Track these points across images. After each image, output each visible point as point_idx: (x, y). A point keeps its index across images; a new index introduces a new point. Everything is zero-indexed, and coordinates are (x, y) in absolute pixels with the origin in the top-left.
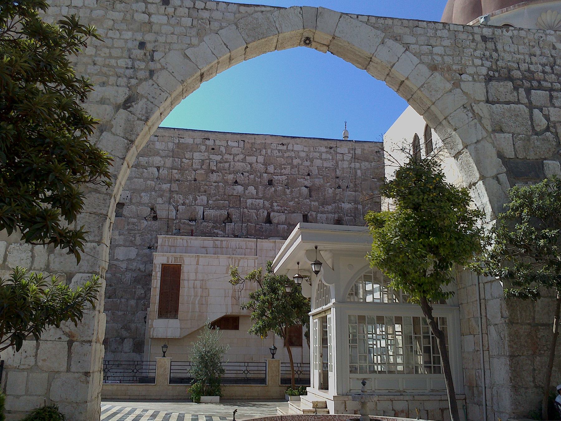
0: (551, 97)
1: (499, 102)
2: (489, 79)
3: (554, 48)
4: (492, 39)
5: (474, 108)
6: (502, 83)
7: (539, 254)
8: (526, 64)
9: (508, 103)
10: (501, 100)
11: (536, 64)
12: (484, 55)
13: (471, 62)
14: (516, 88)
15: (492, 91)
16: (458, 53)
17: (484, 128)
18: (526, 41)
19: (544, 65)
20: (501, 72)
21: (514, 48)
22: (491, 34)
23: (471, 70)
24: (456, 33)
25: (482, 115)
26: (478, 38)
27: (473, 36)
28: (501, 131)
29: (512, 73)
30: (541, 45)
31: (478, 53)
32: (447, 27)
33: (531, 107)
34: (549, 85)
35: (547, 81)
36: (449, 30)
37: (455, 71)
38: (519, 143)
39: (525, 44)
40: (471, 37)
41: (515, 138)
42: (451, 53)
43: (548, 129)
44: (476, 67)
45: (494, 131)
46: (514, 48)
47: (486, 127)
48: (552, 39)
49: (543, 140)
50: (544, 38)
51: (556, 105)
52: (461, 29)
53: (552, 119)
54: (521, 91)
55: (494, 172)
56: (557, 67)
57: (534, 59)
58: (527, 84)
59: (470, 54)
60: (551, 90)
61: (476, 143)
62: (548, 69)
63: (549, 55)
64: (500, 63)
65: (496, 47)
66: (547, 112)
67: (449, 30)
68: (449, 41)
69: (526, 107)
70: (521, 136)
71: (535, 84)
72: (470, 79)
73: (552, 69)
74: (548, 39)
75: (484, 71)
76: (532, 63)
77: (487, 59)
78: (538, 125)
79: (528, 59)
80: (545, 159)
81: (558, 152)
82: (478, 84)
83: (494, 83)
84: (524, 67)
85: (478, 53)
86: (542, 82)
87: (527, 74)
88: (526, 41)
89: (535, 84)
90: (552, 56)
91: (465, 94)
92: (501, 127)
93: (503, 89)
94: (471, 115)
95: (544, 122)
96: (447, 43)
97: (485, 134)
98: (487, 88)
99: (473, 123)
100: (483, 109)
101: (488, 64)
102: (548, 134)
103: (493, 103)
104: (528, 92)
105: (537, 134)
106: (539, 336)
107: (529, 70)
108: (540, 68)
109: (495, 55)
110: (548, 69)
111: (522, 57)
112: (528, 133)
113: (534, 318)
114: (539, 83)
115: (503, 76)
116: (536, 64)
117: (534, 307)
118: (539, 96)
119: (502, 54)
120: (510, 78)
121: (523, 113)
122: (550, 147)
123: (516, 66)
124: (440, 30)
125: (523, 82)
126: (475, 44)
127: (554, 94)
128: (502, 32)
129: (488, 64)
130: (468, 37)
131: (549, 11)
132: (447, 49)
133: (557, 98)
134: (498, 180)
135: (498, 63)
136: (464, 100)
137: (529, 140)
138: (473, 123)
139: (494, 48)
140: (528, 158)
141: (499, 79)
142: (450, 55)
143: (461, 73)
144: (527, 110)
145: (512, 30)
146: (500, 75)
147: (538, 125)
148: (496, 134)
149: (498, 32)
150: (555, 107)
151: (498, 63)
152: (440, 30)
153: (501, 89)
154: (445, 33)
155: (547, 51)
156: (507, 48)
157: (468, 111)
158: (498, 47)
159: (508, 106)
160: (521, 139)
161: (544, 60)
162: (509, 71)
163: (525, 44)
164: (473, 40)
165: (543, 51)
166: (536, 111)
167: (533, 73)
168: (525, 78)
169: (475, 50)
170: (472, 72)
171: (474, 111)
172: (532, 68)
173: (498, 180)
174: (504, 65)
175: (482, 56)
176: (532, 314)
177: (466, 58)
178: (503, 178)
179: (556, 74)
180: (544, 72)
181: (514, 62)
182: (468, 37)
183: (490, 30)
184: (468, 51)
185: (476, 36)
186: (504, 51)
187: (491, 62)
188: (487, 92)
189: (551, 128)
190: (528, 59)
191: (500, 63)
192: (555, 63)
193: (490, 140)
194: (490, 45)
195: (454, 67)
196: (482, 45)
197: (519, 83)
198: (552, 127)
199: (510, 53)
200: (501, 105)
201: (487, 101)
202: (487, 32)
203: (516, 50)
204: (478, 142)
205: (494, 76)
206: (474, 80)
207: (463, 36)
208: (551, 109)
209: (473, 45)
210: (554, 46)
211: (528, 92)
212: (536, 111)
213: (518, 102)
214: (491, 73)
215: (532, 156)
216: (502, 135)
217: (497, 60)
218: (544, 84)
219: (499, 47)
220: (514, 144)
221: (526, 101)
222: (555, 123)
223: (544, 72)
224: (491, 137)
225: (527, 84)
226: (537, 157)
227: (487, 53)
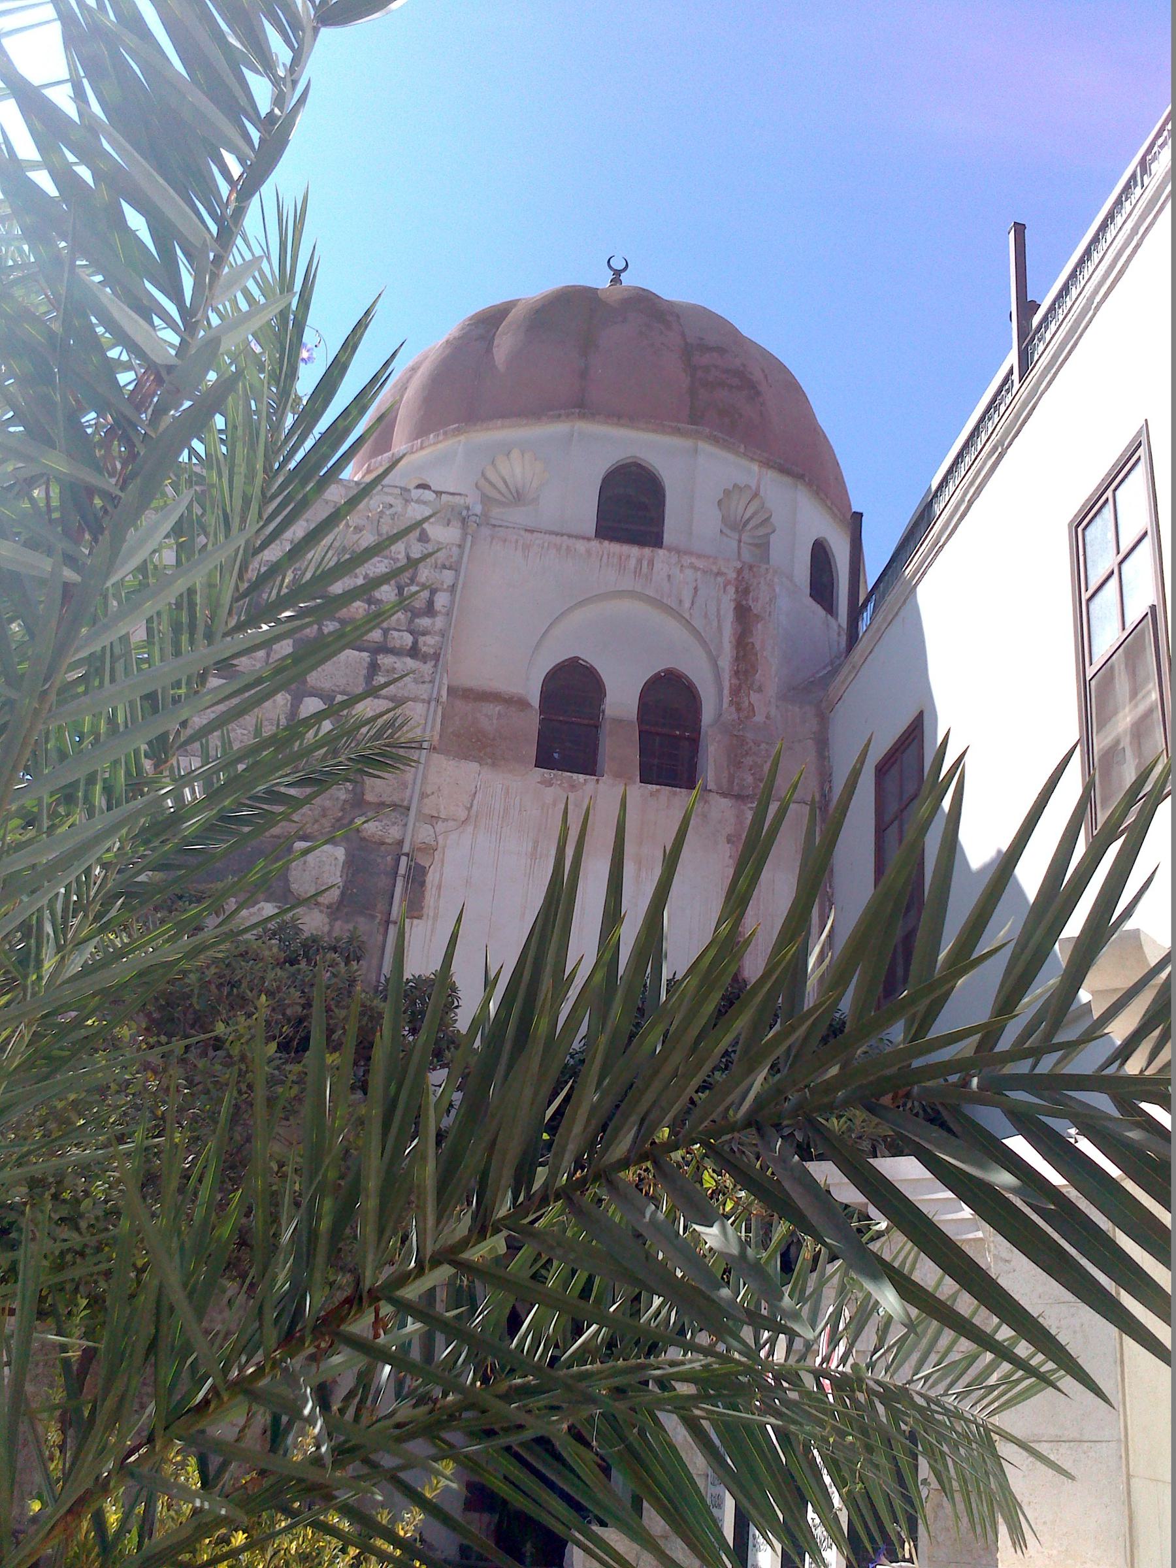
0: (374, 668)
50: (398, 508)
60: (383, 648)
127: (385, 660)
131: (515, 453)
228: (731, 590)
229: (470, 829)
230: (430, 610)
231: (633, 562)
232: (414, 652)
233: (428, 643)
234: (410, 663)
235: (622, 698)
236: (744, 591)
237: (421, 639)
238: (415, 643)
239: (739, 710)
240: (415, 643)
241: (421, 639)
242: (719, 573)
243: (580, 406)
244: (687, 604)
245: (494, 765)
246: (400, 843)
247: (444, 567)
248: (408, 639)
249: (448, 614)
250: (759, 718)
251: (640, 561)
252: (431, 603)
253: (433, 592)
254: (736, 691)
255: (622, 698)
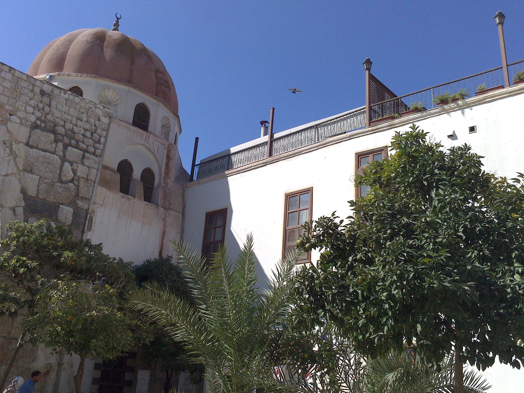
0: (84, 156)
1: (37, 148)
2: (35, 126)
3: (99, 120)
4: (50, 95)
5: (13, 146)
6: (45, 133)
7: (19, 279)
8: (71, 125)
9: (45, 151)
10: (39, 147)
11: (80, 127)
12: (37, 106)
13: (23, 108)
14: (56, 141)
15: (34, 137)
16: (14, 96)
17: (16, 165)
18: (78, 107)
19: (86, 130)
20: (48, 124)
21: (65, 108)
22: (50, 91)
23: (21, 114)
24: (19, 80)
25: (18, 154)
26: (37, 90)
27: (33, 87)
28: (31, 172)
29: (56, 128)
30: (89, 114)
31: (32, 103)
32: (13, 72)
33: (64, 159)
34: (85, 147)
35: (84, 143)
36: (13, 75)
37: (7, 111)
38: (43, 186)
39: (76, 108)
40: (31, 87)
41: (42, 181)
42: (8, 94)
43: (72, 181)
44: (27, 113)
45: (25, 170)
46: (65, 108)
47: (19, 165)
48: (99, 112)
49: (65, 188)
50: (93, 109)
51: (86, 164)
52: (25, 77)
53: (78, 174)
54: (60, 145)
55: (13, 204)
56: (96, 135)
57: (79, 123)
58: (66, 140)
59: (25, 101)
60: (85, 151)
61: (5, 176)
62: (88, 134)
63: (93, 124)
64: (49, 117)
65: (50, 102)
66: (76, 168)
67: (13, 75)
68: (10, 84)
69: (60, 158)
70: (47, 180)
71: (73, 142)
72: (18, 121)
73: (92, 135)
74: (96, 111)
75: (33, 118)
76: (76, 126)
77: (39, 110)
78: (65, 176)
79: (74, 121)
80: (62, 204)
81: (75, 201)
82: (23, 128)
83: (38, 131)
84: (69, 126)
85: (32, 103)
86: (80, 143)
87: (69, 133)
88: (78, 107)
89: (73, 142)
90: (95, 126)
91: (9, 132)
92: (32, 169)
93: (45, 138)
94: (8, 151)
95: (71, 175)
96: (7, 84)
97: (15, 170)
98: (30, 133)
99: (7, 158)
100: (21, 150)
101: (39, 114)
102: (71, 184)
103: (32, 147)
104: (66, 146)
105: (62, 182)
106: (10, 349)
107: (72, 131)
108: (83, 131)
109: (47, 109)
110: (88, 134)
111: (70, 118)
112: (54, 180)
113: (10, 333)
114: (77, 142)
115: (48, 127)
116: (80, 127)
117: (12, 323)
118: (73, 153)
119: (54, 110)
120: (54, 132)
121: (55, 162)
122: (69, 195)
123: (62, 123)
124: (5, 72)
125: (63, 139)
126: (32, 94)
127: (87, 155)
128: (60, 93)
129: (39, 114)
130: (28, 86)
131: (111, 90)
132: (6, 90)
133: (88, 159)
134: (14, 211)
135: (48, 116)
136: (7, 137)
137: (53, 186)
138: (7, 158)
139: (48, 103)
140: (47, 199)
141: (44, 129)
142: (7, 96)
143: (12, 113)
144: (59, 161)
145: (69, 94)
146: (45, 126)
147: (65, 176)
148: (26, 173)
149: (57, 91)
150: (84, 165)
151: (48, 116)
152: (5, 72)
153: (43, 138)
154: (9, 76)
155: (92, 120)
156: (59, 107)
157: (7, 147)
158: (52, 104)
159: (44, 153)
160: (46, 183)
161: (88, 126)
162: (55, 125)
163: (76, 108)
164: (32, 91)
165: (90, 119)
166: (67, 164)
167: (74, 133)
168: (67, 135)
169: (31, 99)
170: (22, 117)
171: (12, 148)
172: (76, 129)
173: (14, 211)
174: (52, 119)
175: (36, 106)
176: (10, 329)
177: (21, 103)
178: (20, 211)
179: (93, 140)
180: (84, 136)
181: (62, 120)
182: (28, 86)
183: (50, 88)
184: (25, 98)
185: (35, 88)
186: (57, 108)
187: (42, 113)
188: (30, 137)
189: (75, 181)
190: (74, 121)
191: (49, 117)
192: (95, 132)
193: (18, 176)
194: (46, 100)
195: (7, 107)
196: (38, 97)
197: (60, 137)
198: (76, 180)
199: (62, 110)
200: (38, 151)
201: (27, 144)
202: (47, 88)
203: (67, 111)
204: (7, 175)
205: (40, 126)
206: (21, 123)
207: (25, 84)
208: (80, 166)
209: (31, 95)
210: (99, 118)
211: (66, 146)
212: (67, 164)
213: (54, 153)
214: (38, 122)
215: (51, 199)
216: (31, 175)
217: (48, 114)
218: (82, 145)
219: (53, 103)
220: (38, 186)
221: (61, 154)
222: (79, 178)
223: (84, 136)
224: (20, 175)
225: (66, 140)
226: (55, 201)
227: (41, 106)
228: (166, 150)
229: (103, 207)
230: (99, 142)
231: (144, 136)
232: (94, 154)
233: (98, 152)
234: (93, 157)
235: (137, 174)
236: (169, 151)
237: (97, 150)
238: (95, 151)
239: (165, 183)
240: (95, 151)
241: (97, 150)
242: (164, 144)
243: (129, 82)
244: (156, 151)
245: (110, 190)
246: (88, 210)
247: (104, 130)
248: (93, 150)
249: (105, 144)
250: (169, 186)
251: (146, 136)
252: (99, 140)
253: (100, 137)
254: (165, 178)
255: (137, 174)
